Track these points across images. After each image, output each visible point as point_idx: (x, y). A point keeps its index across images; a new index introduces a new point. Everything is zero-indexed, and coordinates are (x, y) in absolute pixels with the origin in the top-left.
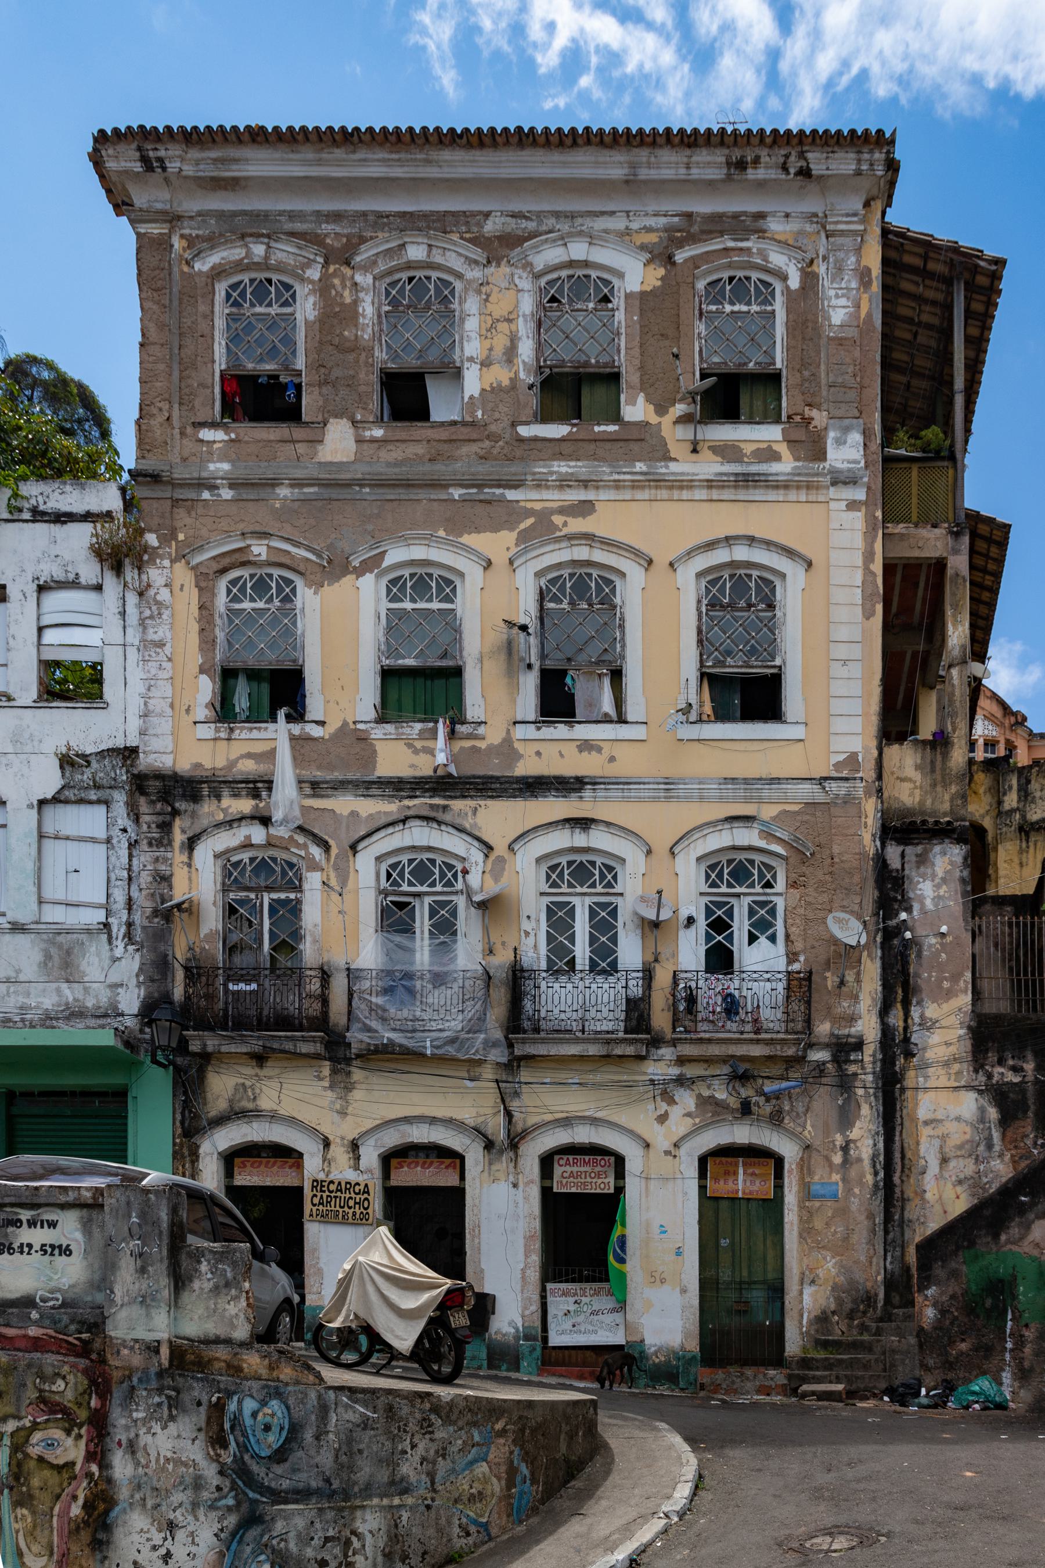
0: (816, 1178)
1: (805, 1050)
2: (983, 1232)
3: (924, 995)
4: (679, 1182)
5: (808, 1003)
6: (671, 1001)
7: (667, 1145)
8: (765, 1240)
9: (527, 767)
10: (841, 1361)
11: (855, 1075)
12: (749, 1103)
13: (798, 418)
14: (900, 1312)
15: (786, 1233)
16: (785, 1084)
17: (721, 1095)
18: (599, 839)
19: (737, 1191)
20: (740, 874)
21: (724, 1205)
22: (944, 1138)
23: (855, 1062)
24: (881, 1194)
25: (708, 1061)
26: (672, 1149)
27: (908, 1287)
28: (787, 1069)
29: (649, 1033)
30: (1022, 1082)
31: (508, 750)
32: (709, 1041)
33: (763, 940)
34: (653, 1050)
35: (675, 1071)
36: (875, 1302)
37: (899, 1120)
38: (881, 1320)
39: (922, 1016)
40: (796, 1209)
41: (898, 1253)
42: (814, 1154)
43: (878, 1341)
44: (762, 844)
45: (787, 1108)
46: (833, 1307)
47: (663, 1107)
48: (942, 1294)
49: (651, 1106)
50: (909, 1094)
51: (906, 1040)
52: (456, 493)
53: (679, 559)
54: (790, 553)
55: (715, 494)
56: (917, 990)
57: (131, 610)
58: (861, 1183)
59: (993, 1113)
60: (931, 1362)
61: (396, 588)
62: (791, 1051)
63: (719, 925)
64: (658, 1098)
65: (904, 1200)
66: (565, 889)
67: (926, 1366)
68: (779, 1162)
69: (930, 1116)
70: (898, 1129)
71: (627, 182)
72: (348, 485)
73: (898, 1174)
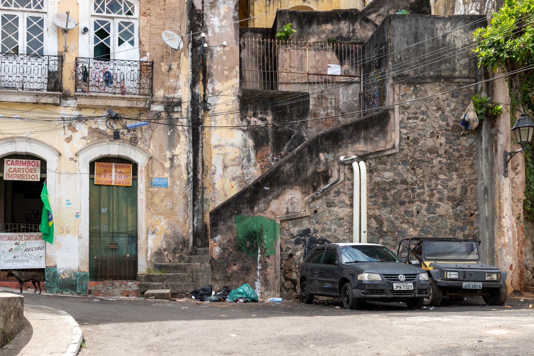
0: (156, 175)
1: (150, 104)
2: (245, 206)
3: (214, 78)
4: (78, 176)
5: (152, 79)
6: (74, 74)
7: (71, 155)
8: (127, 209)
10: (168, 277)
11: (177, 119)
12: (118, 133)
14: (201, 249)
15: (139, 205)
16: (138, 123)
17: (103, 127)
19: (111, 182)
21: (104, 189)
22: (225, 155)
23: (177, 112)
24: (191, 184)
25: (95, 108)
26: (74, 157)
27: (206, 236)
28: (139, 115)
29: (61, 91)
32: (96, 97)
34: (63, 101)
35: (76, 113)
36: (188, 244)
37: (201, 144)
38: (191, 254)
39: (213, 89)
40: (144, 192)
41: (200, 217)
42: (155, 162)
43: (189, 265)
45: (140, 136)
46: (164, 247)
47: (69, 133)
48: (223, 239)
49: (62, 132)
50: (206, 130)
51: (205, 101)
56: (211, 75)
58: (180, 178)
59: (251, 143)
60: (218, 277)
62: (142, 105)
64: (66, 128)
65: (203, 188)
67: (215, 279)
68: (135, 166)
69: (217, 143)
70: (200, 149)
73: (200, 174)
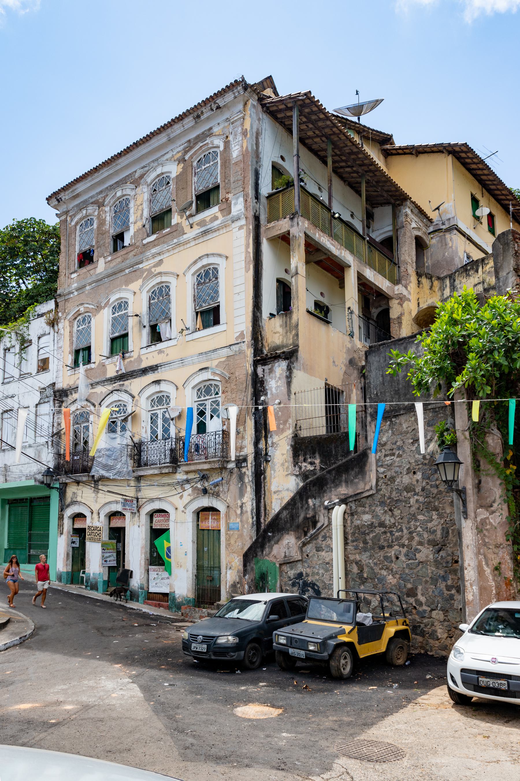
9: (144, 365)
13: (224, 200)
20: (208, 391)
31: (139, 360)
33: (215, 417)
44: (212, 377)
51: (266, 454)
52: (127, 271)
53: (186, 271)
54: (220, 255)
55: (197, 242)
63: (202, 413)
66: (155, 408)
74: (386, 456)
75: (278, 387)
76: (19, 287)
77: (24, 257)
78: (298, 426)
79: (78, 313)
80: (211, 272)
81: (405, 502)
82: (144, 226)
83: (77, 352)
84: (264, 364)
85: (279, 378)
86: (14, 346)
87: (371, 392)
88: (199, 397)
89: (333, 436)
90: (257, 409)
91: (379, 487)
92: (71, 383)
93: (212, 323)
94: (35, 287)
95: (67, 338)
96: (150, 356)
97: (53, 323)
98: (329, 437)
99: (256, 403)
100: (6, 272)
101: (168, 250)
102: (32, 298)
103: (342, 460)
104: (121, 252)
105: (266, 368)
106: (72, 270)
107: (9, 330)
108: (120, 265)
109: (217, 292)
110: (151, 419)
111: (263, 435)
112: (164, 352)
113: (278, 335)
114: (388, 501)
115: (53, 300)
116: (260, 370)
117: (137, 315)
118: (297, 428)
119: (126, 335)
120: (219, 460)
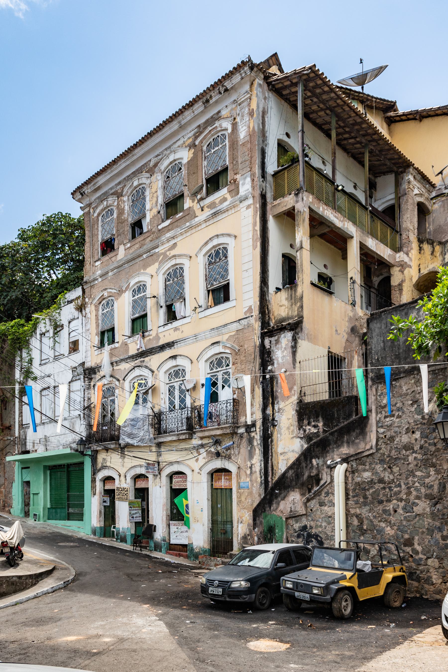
3: (279, 399)
9: (161, 343)
18: (180, 361)
20: (219, 363)
23: (253, 431)
24: (263, 485)
30: (318, 432)
31: (157, 338)
33: (226, 387)
37: (270, 454)
44: (223, 351)
51: (273, 419)
52: (145, 256)
53: (198, 252)
56: (277, 398)
57: (84, 322)
58: (256, 482)
61: (135, 292)
63: (214, 384)
71: (180, 127)
72: (122, 266)
74: (386, 417)
75: (284, 356)
76: (51, 277)
77: (54, 249)
78: (303, 393)
79: (103, 298)
80: (221, 252)
81: (404, 459)
82: (159, 212)
83: (103, 333)
84: (271, 336)
85: (285, 348)
86: (48, 331)
87: (372, 358)
88: (212, 369)
89: (335, 400)
90: (264, 377)
91: (379, 447)
92: (98, 362)
93: (223, 300)
94: (64, 276)
95: (94, 321)
96: (166, 334)
97: (81, 308)
98: (332, 401)
99: (264, 372)
100: (39, 264)
101: (181, 234)
102: (62, 286)
103: (343, 422)
104: (139, 239)
105: (273, 339)
106: (96, 258)
107: (44, 317)
108: (139, 251)
109: (227, 271)
110: (169, 391)
111: (271, 402)
112: (179, 329)
113: (283, 308)
114: (388, 459)
115: (81, 287)
116: (267, 341)
117: (154, 297)
118: (302, 394)
119: (145, 316)
120: (230, 426)
